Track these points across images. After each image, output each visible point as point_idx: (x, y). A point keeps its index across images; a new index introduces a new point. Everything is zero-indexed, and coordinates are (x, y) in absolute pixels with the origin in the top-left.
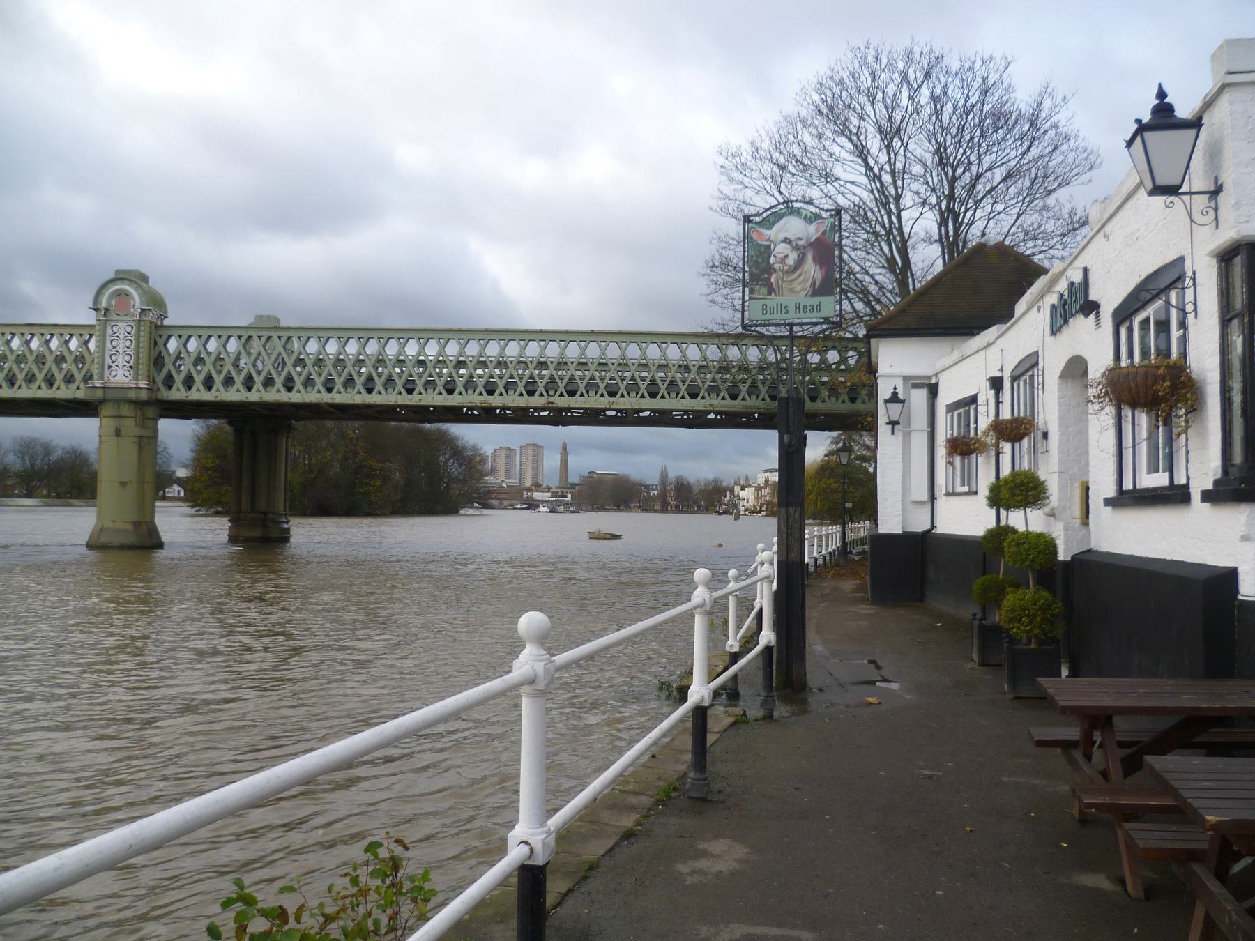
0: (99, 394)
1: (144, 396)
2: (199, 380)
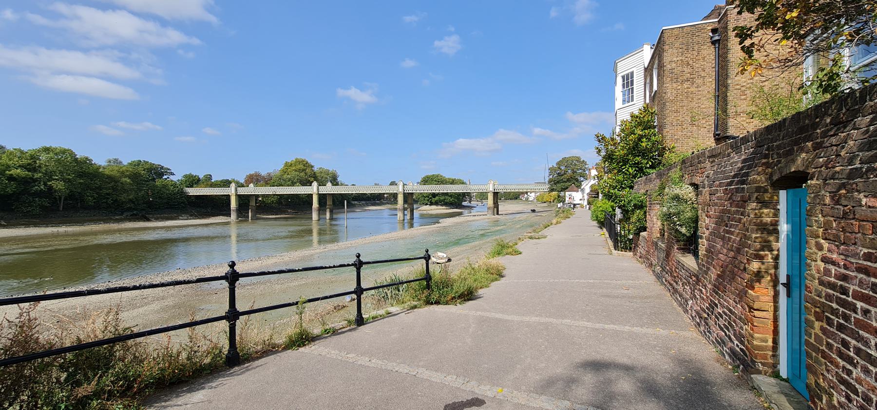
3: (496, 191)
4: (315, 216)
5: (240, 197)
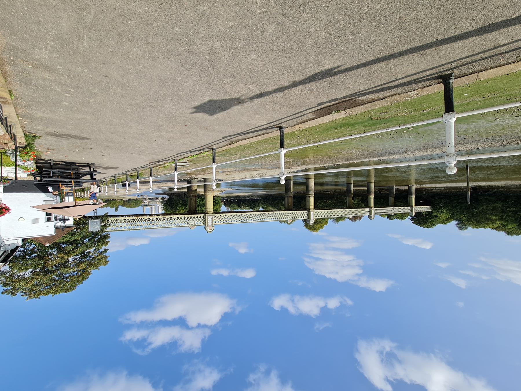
0: (213, 214)
1: (206, 215)
2: (199, 218)
3: (202, 215)
4: (373, 186)
5: (407, 204)
